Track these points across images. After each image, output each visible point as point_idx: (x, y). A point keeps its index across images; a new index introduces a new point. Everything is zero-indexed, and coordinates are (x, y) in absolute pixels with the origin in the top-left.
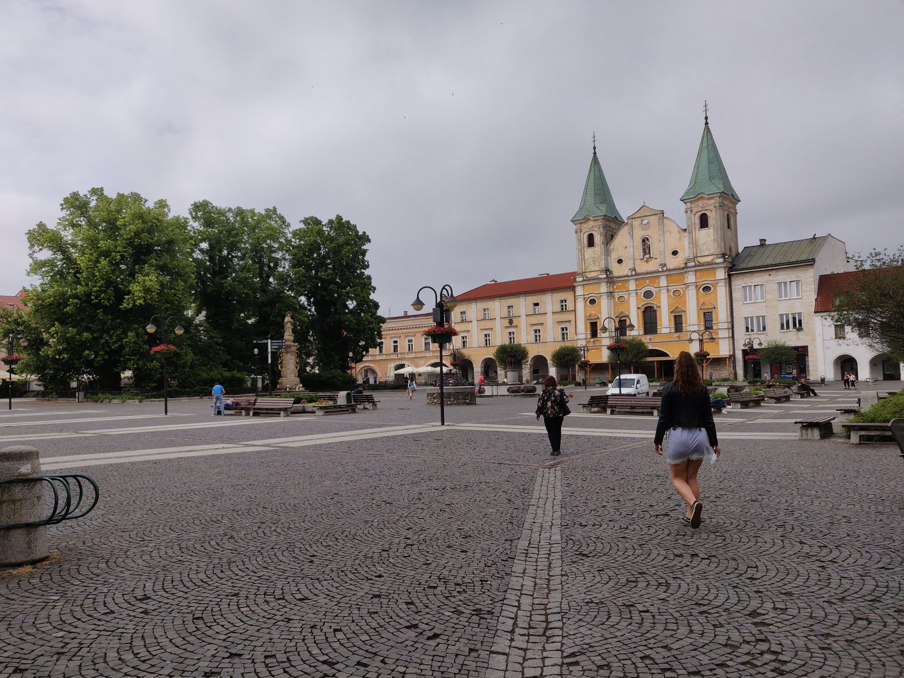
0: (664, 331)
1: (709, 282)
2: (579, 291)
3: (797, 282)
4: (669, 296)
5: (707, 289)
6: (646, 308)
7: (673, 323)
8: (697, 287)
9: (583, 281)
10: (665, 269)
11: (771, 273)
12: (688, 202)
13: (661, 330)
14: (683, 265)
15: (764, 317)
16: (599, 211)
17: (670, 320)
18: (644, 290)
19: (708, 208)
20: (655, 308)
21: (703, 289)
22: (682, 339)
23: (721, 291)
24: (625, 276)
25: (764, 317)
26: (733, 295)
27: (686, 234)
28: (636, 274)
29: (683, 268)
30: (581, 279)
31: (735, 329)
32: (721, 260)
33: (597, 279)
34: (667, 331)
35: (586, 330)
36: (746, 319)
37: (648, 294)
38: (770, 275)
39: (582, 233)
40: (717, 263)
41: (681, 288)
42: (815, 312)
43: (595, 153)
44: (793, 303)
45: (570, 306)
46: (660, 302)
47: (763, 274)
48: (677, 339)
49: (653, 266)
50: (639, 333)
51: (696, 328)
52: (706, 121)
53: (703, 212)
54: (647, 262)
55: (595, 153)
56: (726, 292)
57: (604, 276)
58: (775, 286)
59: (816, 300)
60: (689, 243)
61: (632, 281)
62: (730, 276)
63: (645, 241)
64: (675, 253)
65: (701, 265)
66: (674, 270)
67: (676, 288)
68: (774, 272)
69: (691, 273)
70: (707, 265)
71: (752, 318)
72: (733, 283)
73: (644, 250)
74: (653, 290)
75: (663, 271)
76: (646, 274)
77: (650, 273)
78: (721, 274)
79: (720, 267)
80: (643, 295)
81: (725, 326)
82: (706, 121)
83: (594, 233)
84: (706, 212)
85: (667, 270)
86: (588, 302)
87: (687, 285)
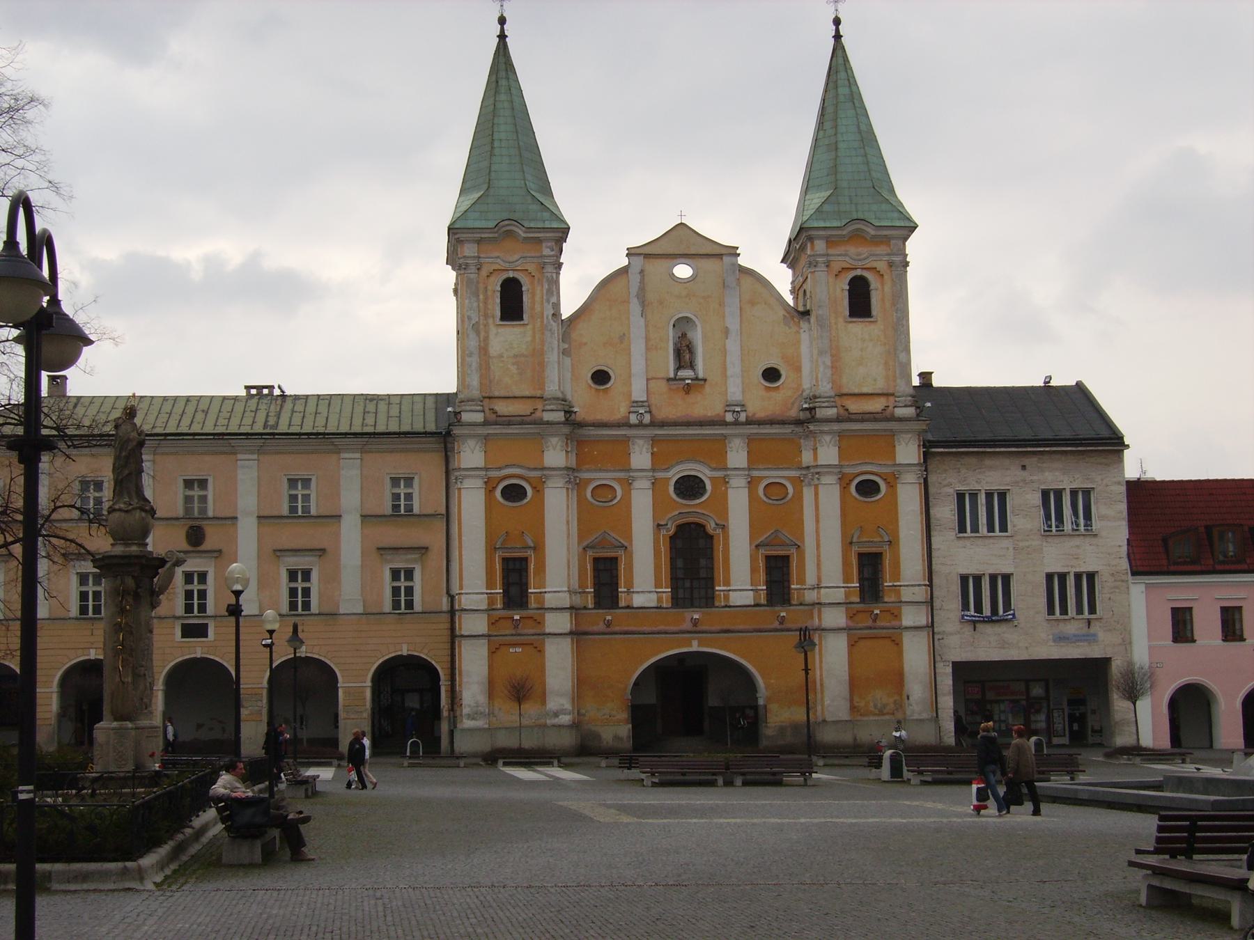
0: (738, 599)
1: (874, 469)
2: (470, 455)
3: (1087, 493)
4: (752, 497)
5: (868, 488)
6: (680, 527)
7: (762, 576)
8: (844, 481)
9: (486, 423)
10: (743, 417)
11: (1026, 461)
12: (820, 238)
13: (727, 598)
14: (793, 413)
15: (1007, 578)
16: (546, 215)
17: (754, 570)
18: (675, 474)
19: (875, 265)
20: (711, 527)
21: (504, 492)
22: (617, 629)
23: (908, 498)
24: (619, 425)
25: (1007, 578)
26: (932, 512)
27: (804, 325)
28: (653, 424)
29: (798, 422)
30: (479, 417)
31: (937, 604)
32: (910, 412)
33: (534, 423)
34: (746, 598)
35: (490, 584)
36: (964, 579)
37: (690, 487)
38: (1024, 467)
39: (484, 273)
40: (900, 420)
41: (788, 478)
42: (1134, 573)
43: (502, 37)
44: (1078, 546)
45: (424, 497)
46: (724, 511)
47: (1006, 462)
48: (776, 625)
49: (706, 405)
50: (660, 600)
51: (839, 596)
52: (837, 30)
53: (859, 272)
54: (688, 389)
55: (502, 37)
56: (921, 502)
57: (560, 416)
58: (1037, 499)
59: (1128, 540)
60: (821, 353)
61: (640, 442)
62: (926, 456)
63: (683, 324)
64: (771, 375)
65: (848, 417)
66: (771, 422)
67: (774, 475)
68: (1034, 459)
69: (828, 438)
70: (875, 420)
71: (978, 579)
72: (932, 479)
73: (678, 353)
74: (705, 473)
75: (736, 423)
76: (688, 424)
77: (701, 423)
78: (908, 452)
79: (907, 432)
80: (671, 489)
81: (921, 594)
82: (837, 30)
83: (522, 278)
84: (866, 274)
85: (749, 422)
86: (498, 493)
87: (814, 472)
